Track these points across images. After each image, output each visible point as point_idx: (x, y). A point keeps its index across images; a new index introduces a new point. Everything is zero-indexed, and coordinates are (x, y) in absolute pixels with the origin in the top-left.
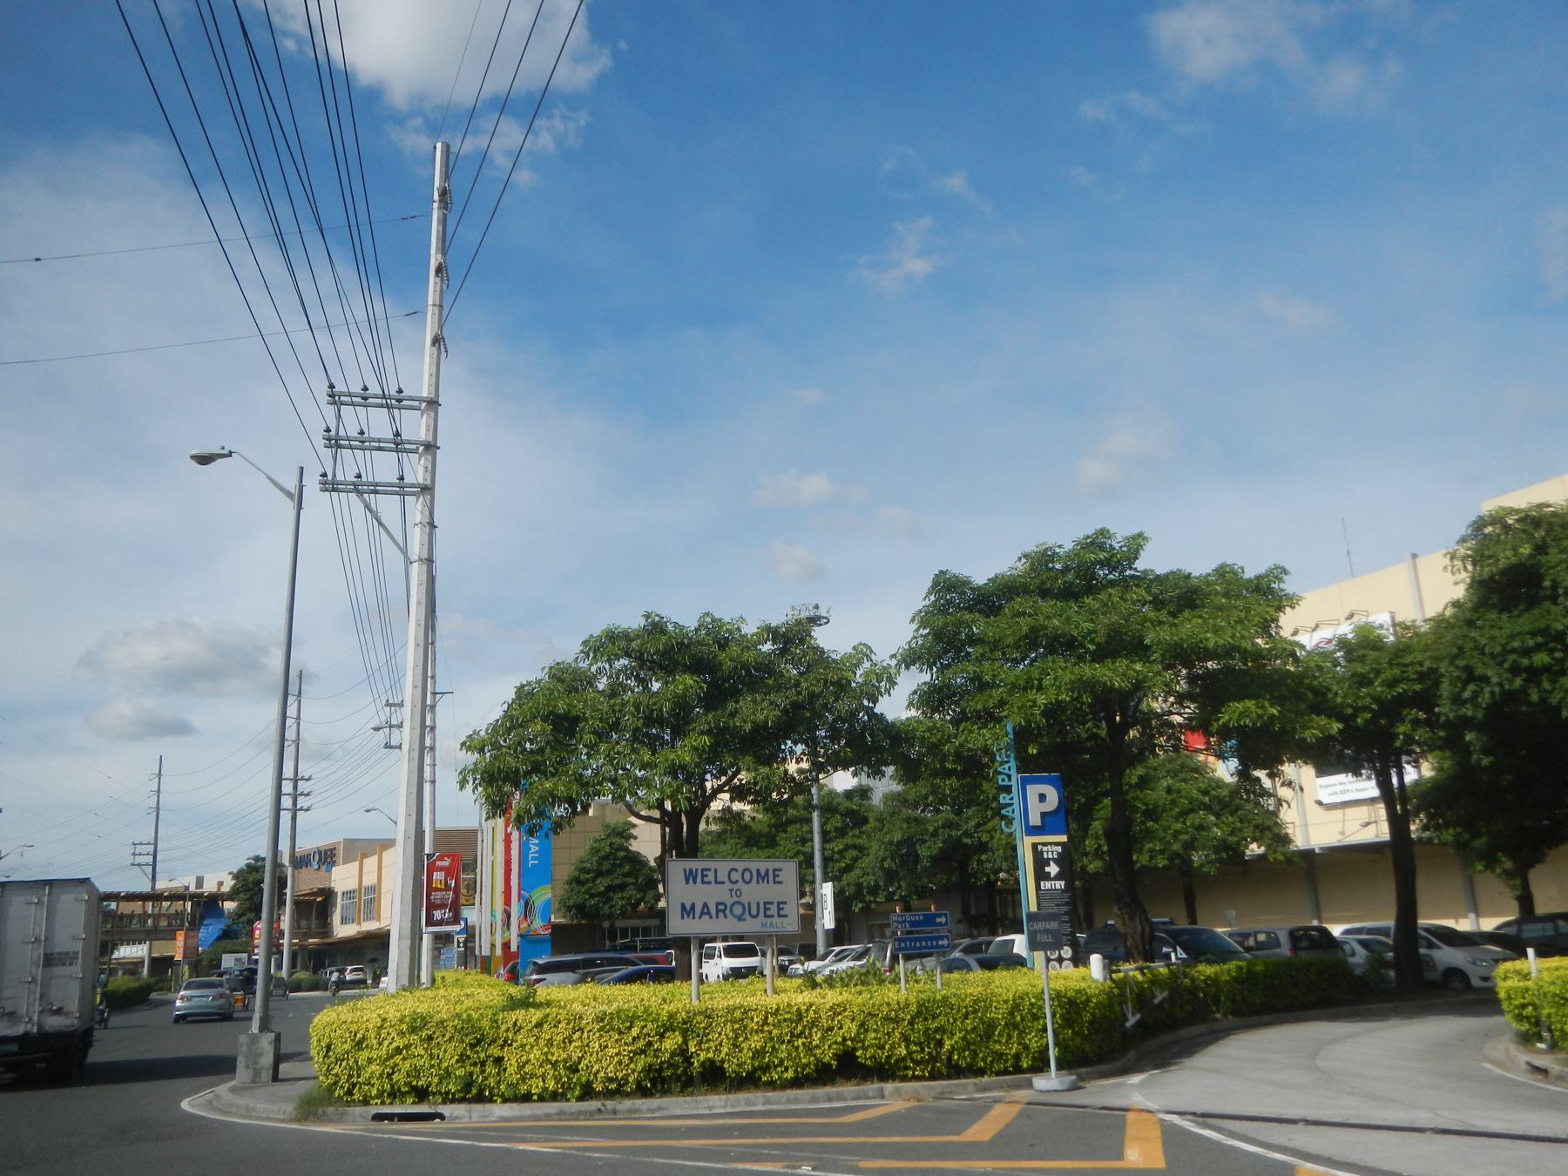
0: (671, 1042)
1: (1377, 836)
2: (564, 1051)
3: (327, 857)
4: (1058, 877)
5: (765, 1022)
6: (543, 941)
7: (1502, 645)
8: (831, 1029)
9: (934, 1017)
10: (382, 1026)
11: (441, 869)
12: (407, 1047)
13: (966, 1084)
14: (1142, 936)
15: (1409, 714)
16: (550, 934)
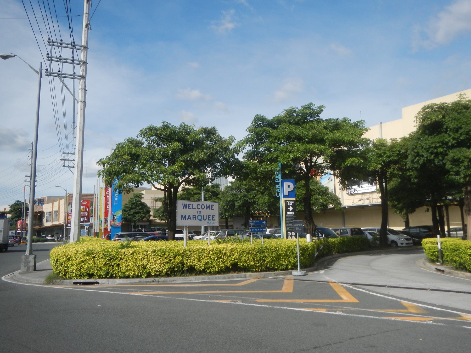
0: (178, 260)
1: (363, 203)
2: (141, 262)
3: (42, 202)
4: (292, 211)
5: (209, 253)
6: (119, 228)
7: (429, 146)
8: (230, 256)
9: (263, 253)
10: (77, 253)
12: (86, 260)
13: (272, 273)
14: (313, 229)
15: (393, 166)
16: (121, 226)
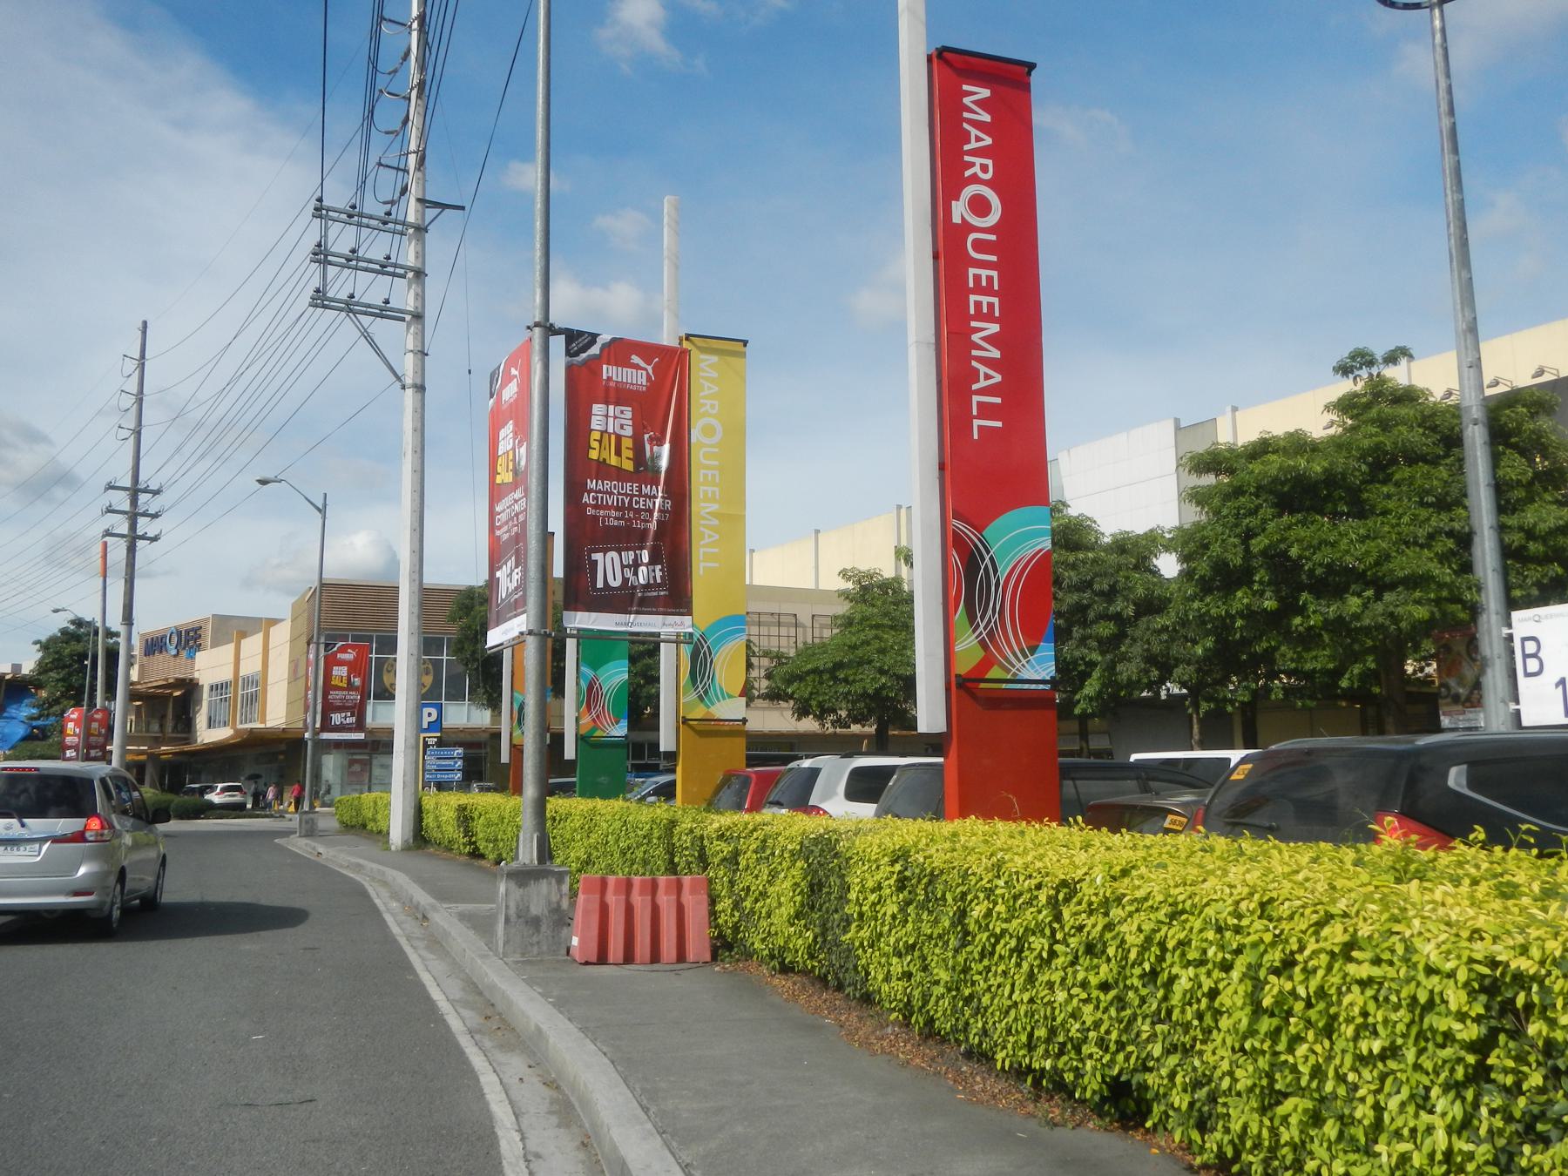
3: (190, 639)
11: (618, 395)
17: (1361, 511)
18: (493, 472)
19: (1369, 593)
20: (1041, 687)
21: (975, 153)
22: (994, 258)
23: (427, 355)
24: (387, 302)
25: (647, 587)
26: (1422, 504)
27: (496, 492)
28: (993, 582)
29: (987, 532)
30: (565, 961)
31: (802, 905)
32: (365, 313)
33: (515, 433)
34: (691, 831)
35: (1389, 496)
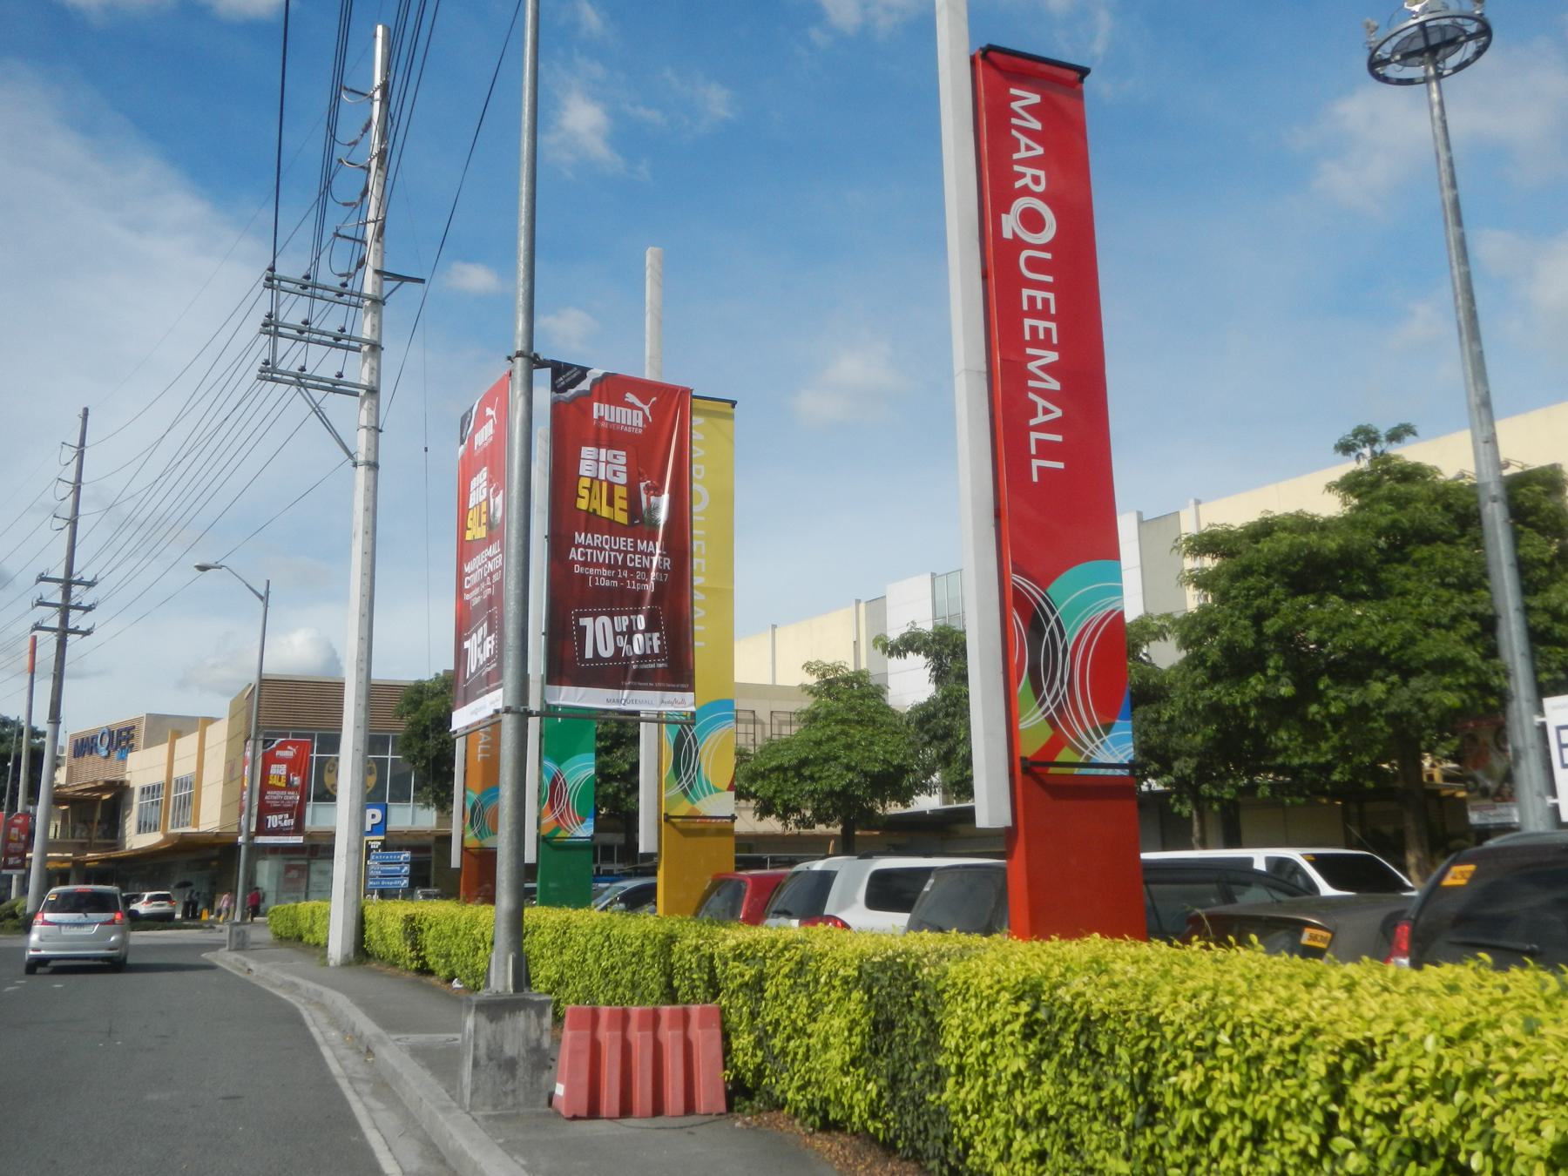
3: (122, 740)
11: (611, 438)
17: (1380, 592)
18: (462, 527)
19: (1394, 678)
20: (1119, 772)
21: (1025, 162)
22: (1049, 279)
23: (381, 431)
24: (340, 375)
25: (643, 657)
26: (1443, 585)
27: (465, 551)
28: (1060, 647)
29: (1049, 590)
30: (547, 1115)
31: (863, 1048)
32: (316, 387)
33: (490, 481)
34: (697, 948)
35: (1407, 577)
